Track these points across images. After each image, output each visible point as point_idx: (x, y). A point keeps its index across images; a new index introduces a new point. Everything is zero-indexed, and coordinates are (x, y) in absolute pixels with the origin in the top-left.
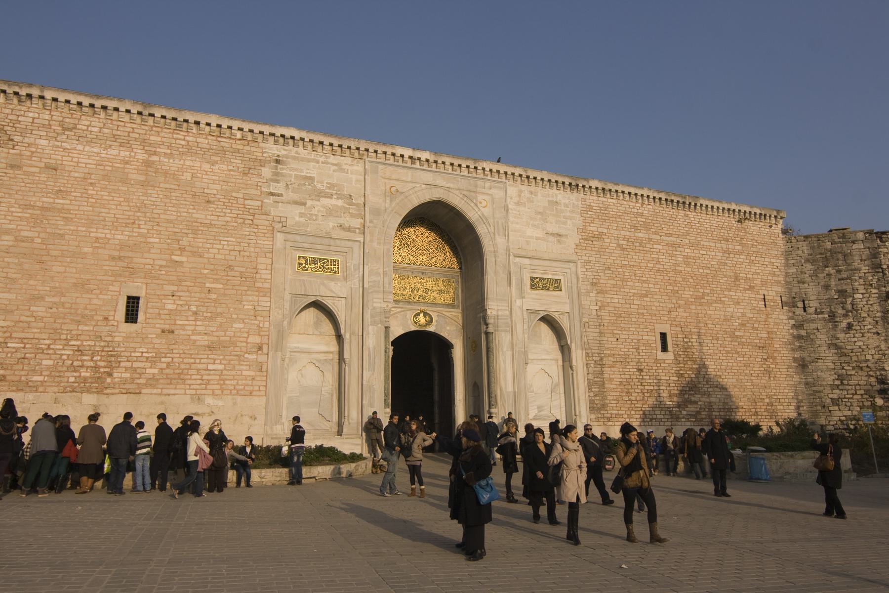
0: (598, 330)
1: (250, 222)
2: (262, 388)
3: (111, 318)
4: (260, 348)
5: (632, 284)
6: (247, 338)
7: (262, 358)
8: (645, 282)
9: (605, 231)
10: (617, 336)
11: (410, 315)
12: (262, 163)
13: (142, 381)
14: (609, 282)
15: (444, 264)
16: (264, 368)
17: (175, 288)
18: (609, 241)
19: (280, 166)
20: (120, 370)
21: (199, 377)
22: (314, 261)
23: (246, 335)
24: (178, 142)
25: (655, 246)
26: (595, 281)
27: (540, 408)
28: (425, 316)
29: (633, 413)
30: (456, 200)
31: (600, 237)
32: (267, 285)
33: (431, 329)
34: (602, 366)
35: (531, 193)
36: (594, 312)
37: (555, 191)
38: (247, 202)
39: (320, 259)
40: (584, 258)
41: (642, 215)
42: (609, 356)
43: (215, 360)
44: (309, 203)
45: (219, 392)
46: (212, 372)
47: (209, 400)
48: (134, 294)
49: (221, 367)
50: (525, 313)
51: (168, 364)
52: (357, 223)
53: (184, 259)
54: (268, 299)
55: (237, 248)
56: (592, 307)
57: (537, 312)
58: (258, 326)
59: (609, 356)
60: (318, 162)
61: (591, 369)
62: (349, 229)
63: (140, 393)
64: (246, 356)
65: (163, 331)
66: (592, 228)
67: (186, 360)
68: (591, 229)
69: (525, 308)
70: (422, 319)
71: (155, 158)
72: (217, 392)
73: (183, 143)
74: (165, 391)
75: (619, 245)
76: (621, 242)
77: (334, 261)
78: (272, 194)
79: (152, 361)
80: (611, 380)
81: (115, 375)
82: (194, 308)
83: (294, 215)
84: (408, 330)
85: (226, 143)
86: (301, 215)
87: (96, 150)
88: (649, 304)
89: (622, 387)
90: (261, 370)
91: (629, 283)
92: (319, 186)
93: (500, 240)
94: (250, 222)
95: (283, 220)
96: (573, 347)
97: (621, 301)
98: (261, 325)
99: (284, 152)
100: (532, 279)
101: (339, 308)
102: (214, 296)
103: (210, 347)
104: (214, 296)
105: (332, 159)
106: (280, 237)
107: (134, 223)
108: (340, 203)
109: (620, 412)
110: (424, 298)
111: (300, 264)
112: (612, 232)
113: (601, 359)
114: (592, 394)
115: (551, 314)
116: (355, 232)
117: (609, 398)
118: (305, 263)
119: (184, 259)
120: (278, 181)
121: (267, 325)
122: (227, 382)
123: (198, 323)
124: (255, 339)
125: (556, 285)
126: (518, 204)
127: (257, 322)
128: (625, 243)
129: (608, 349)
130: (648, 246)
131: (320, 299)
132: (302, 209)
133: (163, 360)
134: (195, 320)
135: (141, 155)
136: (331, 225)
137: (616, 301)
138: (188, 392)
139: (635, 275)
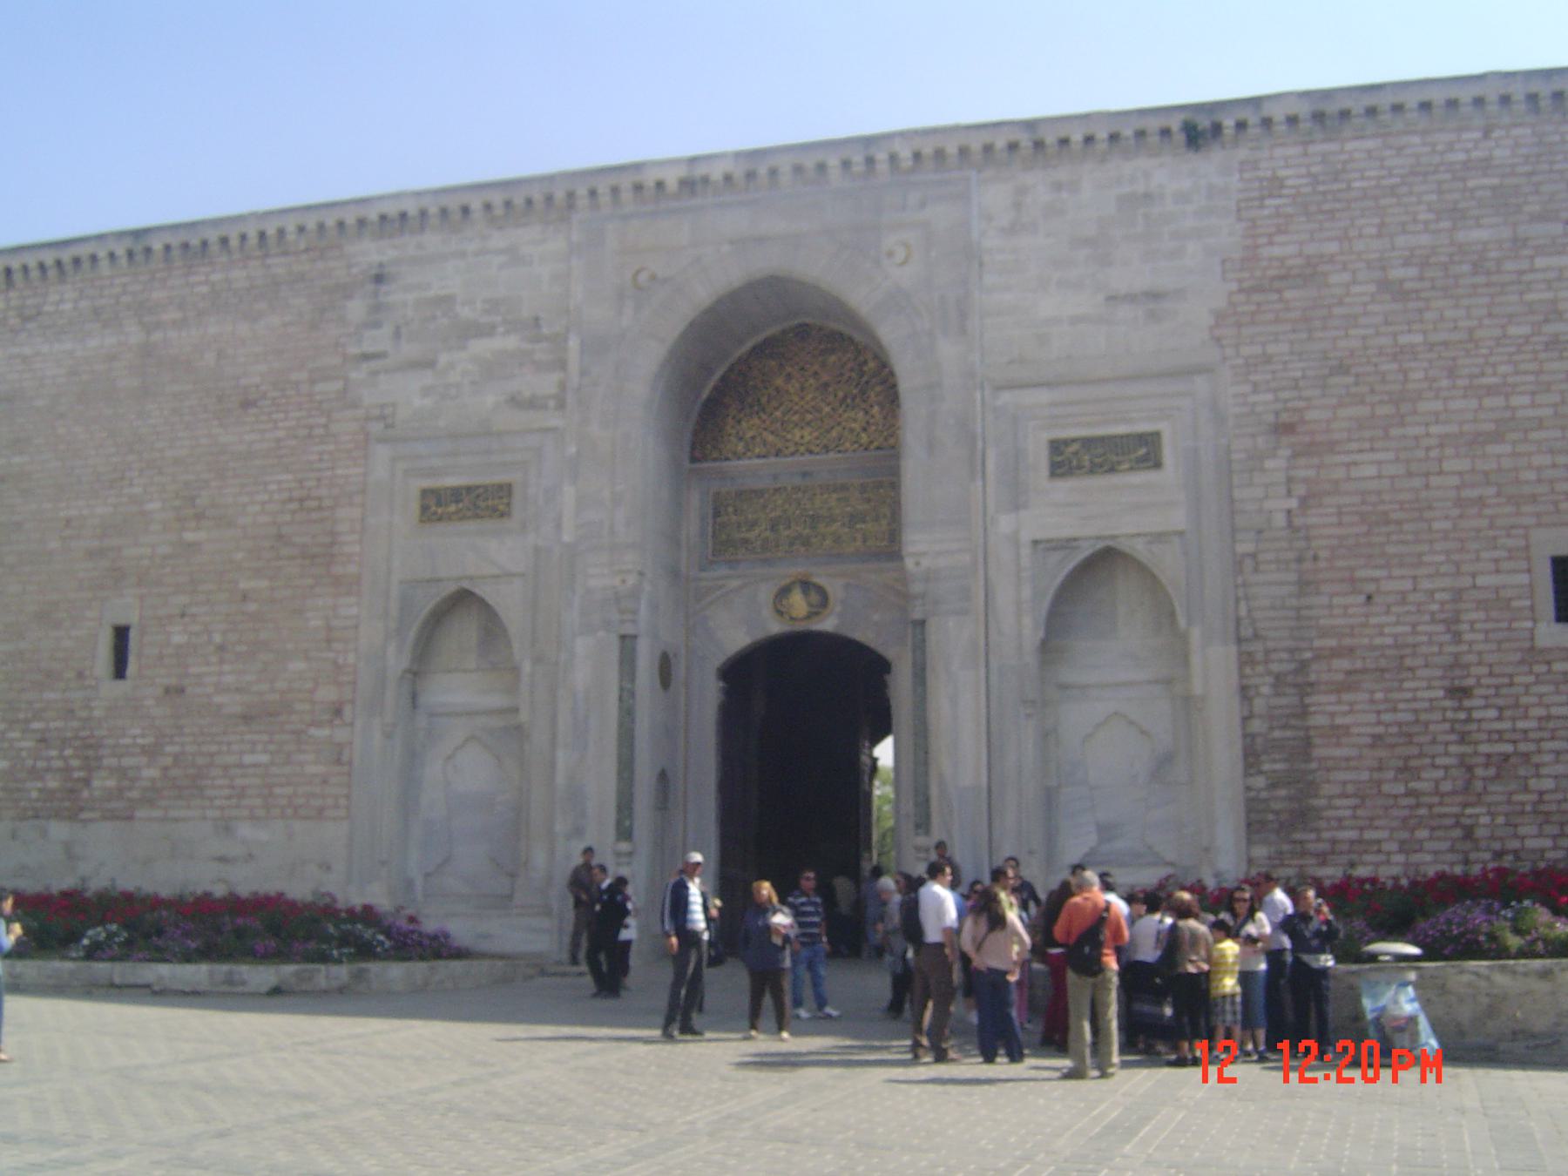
0: (1293, 577)
1: (321, 431)
2: (343, 802)
3: (87, 673)
4: (338, 712)
5: (1437, 406)
6: (312, 691)
7: (341, 735)
8: (1491, 391)
9: (1332, 247)
10: (1371, 588)
11: (766, 593)
12: (345, 291)
13: (135, 794)
14: (1344, 412)
15: (864, 438)
16: (345, 758)
17: (183, 599)
18: (1346, 277)
19: (384, 288)
20: (103, 774)
21: (225, 782)
22: (456, 494)
23: (309, 685)
24: (197, 290)
25: (1540, 262)
26: (1285, 417)
27: (1106, 831)
29: (1422, 834)
30: (817, 266)
31: (1310, 272)
32: (352, 569)
33: (828, 624)
34: (1305, 689)
35: (1058, 186)
36: (1280, 520)
37: (1143, 163)
38: (319, 387)
39: (469, 489)
40: (1246, 351)
41: (1486, 166)
42: (1336, 653)
43: (254, 743)
44: (443, 359)
45: (261, 813)
46: (251, 771)
47: (245, 830)
48: (122, 621)
49: (264, 758)
50: (1026, 551)
51: (176, 757)
52: (547, 384)
53: (201, 536)
54: (353, 599)
55: (296, 494)
56: (1268, 505)
57: (1068, 544)
58: (335, 663)
59: (1336, 653)
60: (463, 255)
61: (1259, 705)
62: (533, 404)
63: (130, 818)
64: (313, 731)
65: (167, 691)
66: (1284, 248)
67: (205, 749)
68: (1277, 251)
69: (1026, 536)
70: (798, 603)
71: (157, 336)
72: (261, 813)
73: (204, 289)
74: (173, 813)
75: (1384, 285)
76: (1396, 273)
77: (500, 487)
78: (366, 357)
79: (152, 752)
80: (1337, 733)
81: (96, 783)
82: (218, 638)
83: (409, 394)
84: (760, 635)
85: (279, 266)
86: (426, 391)
87: (68, 346)
88: (1507, 463)
89: (1382, 753)
90: (338, 762)
91: (1423, 406)
92: (465, 313)
93: (948, 350)
94: (321, 431)
95: (388, 411)
96: (1196, 634)
97: (1392, 470)
98: (341, 661)
99: (391, 254)
100: (1056, 446)
101: (508, 602)
102: (252, 607)
103: (246, 718)
104: (252, 607)
105: (498, 240)
106: (382, 453)
107: (122, 478)
108: (512, 342)
109: (1369, 835)
110: (806, 543)
111: (424, 509)
112: (1359, 246)
113: (1303, 666)
114: (1260, 782)
115: (1124, 545)
116: (545, 407)
117: (1327, 789)
118: (441, 505)
119: (201, 536)
120: (377, 325)
121: (351, 658)
122: (277, 791)
123: (226, 668)
124: (327, 694)
125: (1143, 451)
126: (1012, 230)
127: (331, 655)
128: (1412, 272)
129: (1324, 633)
130: (1509, 266)
131: (466, 585)
132: (428, 378)
133: (169, 749)
134: (222, 662)
135: (135, 335)
136: (490, 400)
137: (1371, 471)
138: (210, 813)
139: (1452, 373)
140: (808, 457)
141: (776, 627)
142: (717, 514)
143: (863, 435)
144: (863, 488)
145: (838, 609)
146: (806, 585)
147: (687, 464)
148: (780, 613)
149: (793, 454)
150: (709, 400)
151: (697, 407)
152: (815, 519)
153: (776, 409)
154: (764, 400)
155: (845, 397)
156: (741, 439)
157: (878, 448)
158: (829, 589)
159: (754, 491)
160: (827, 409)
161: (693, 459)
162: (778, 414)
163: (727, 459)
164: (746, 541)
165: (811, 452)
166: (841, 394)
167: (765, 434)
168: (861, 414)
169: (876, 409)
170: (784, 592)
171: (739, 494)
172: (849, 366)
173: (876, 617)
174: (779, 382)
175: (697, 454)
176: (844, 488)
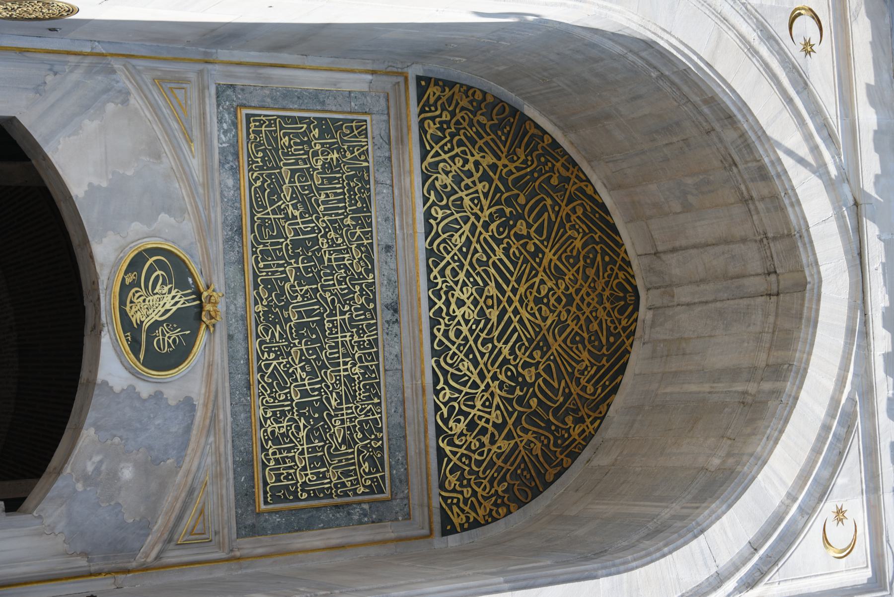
11: (174, 232)
28: (177, 318)
70: (159, 303)
110: (271, 318)
140: (426, 314)
141: (107, 252)
142: (327, 127)
143: (462, 426)
144: (371, 428)
145: (145, 389)
146: (191, 319)
147: (414, 71)
148: (136, 264)
149: (432, 284)
150: (525, 118)
151: (512, 97)
152: (312, 331)
153: (506, 251)
154: (521, 227)
155: (524, 384)
156: (458, 180)
157: (441, 453)
158: (183, 368)
159: (367, 201)
160: (506, 352)
161: (424, 83)
162: (500, 253)
163: (424, 155)
164: (275, 192)
165: (434, 322)
166: (529, 375)
167: (466, 228)
168: (495, 417)
169: (505, 445)
170: (176, 270)
171: (361, 176)
172: (575, 389)
173: (127, 473)
174: (549, 255)
175: (433, 91)
176: (373, 390)
